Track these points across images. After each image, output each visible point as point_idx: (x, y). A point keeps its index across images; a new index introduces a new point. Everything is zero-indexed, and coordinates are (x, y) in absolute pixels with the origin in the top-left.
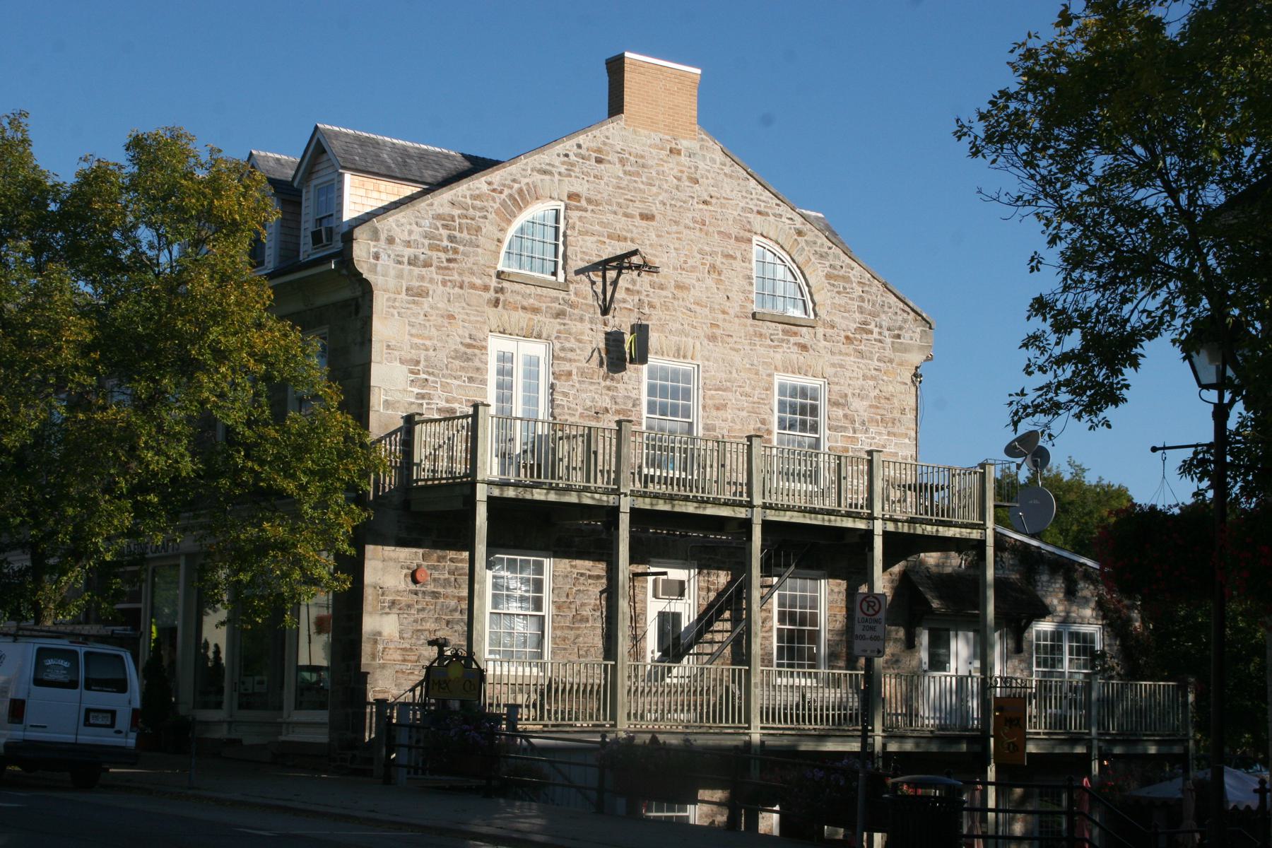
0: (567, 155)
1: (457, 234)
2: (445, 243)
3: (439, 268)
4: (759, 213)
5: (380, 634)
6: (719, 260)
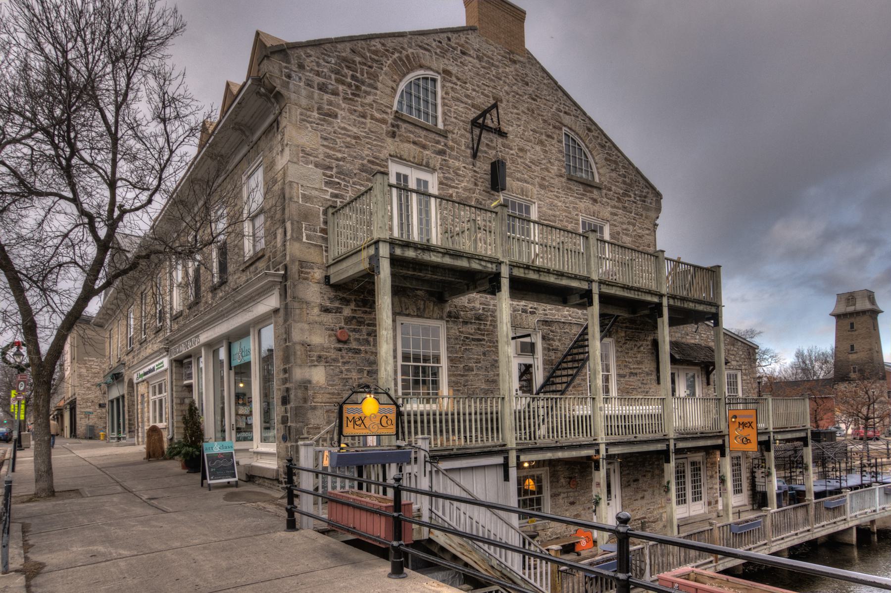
0: (440, 42)
1: (358, 75)
2: (349, 80)
3: (345, 99)
4: (565, 113)
5: (310, 382)
6: (544, 137)
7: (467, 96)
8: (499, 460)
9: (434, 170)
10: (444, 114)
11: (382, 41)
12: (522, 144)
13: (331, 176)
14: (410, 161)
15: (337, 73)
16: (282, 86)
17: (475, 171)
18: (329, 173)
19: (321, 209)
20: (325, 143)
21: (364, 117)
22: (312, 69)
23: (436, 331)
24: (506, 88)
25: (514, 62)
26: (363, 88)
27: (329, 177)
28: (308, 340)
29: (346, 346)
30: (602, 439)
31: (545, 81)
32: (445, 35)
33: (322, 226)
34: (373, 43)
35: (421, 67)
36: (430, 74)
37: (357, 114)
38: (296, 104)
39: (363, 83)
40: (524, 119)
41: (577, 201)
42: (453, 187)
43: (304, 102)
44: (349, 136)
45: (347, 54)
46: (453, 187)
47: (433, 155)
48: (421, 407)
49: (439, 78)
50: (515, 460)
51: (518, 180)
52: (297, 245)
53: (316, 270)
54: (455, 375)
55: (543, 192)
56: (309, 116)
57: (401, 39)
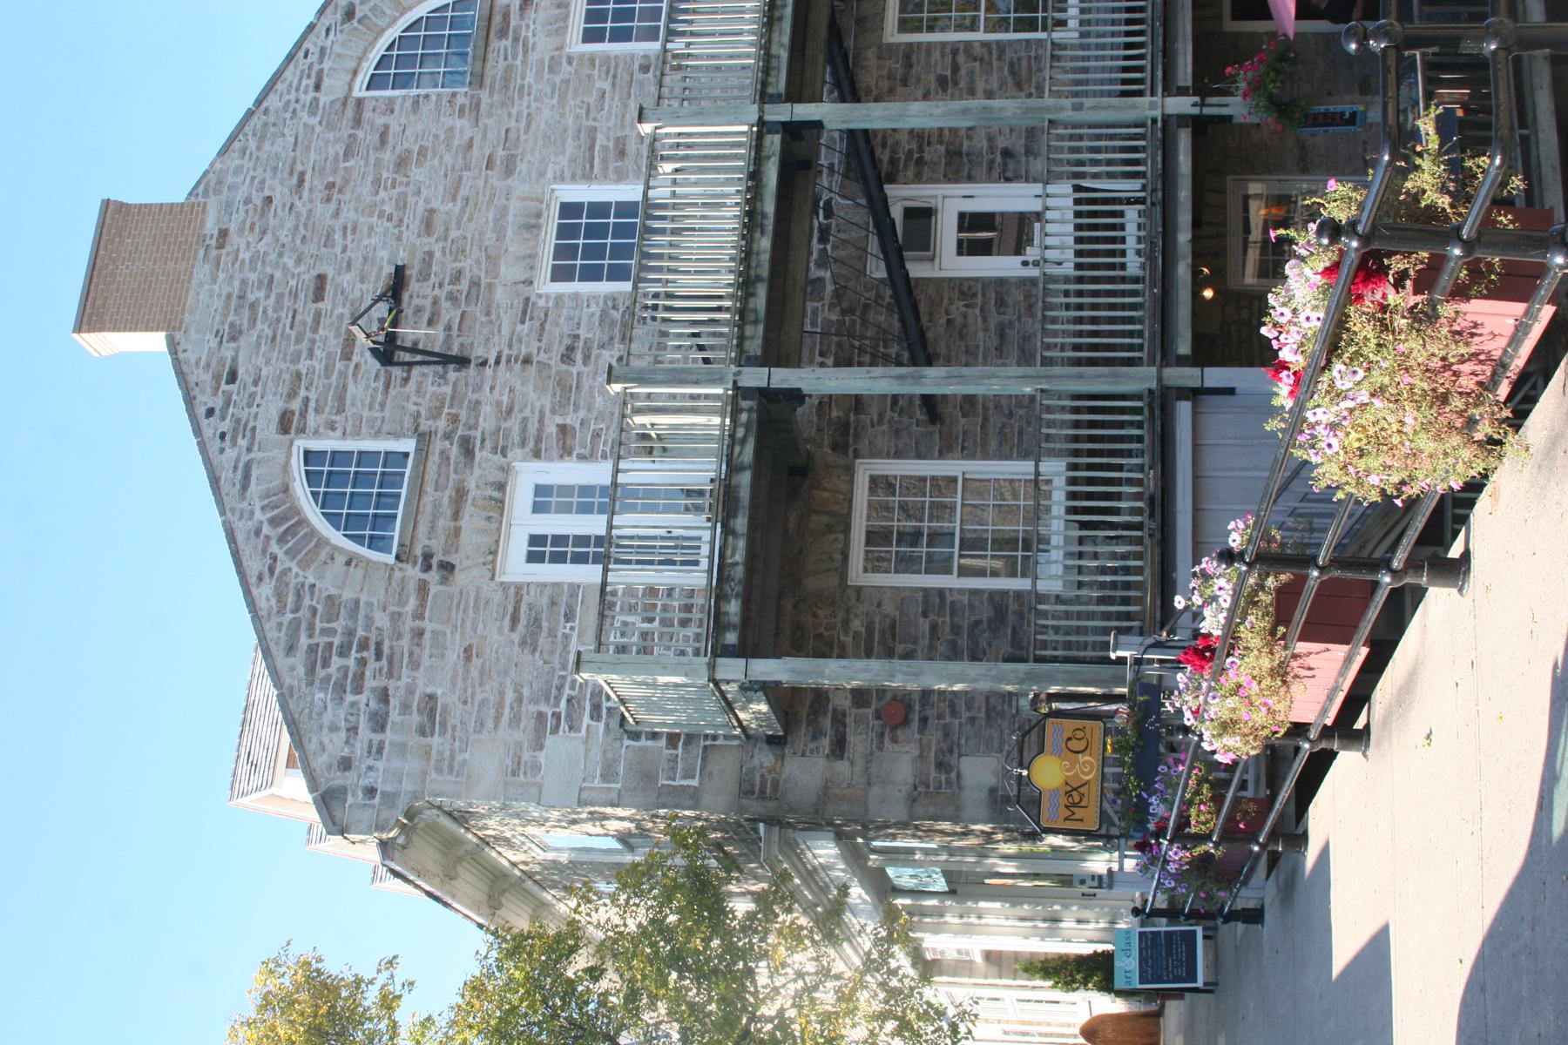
0: (223, 436)
1: (337, 641)
2: (351, 662)
3: (390, 675)
4: (317, 87)
5: (993, 791)
6: (388, 156)
7: (328, 371)
8: (1184, 409)
9: (506, 470)
10: (377, 434)
11: (254, 580)
12: (413, 225)
13: (557, 716)
14: (499, 529)
15: (340, 688)
16: (392, 806)
17: (497, 362)
18: (550, 721)
19: (627, 742)
20: (490, 724)
21: (420, 633)
22: (347, 742)
23: (879, 484)
24: (289, 262)
25: (223, 234)
26: (360, 633)
27: (559, 719)
28: (905, 789)
29: (917, 707)
30: (1152, 106)
31: (253, 144)
32: (204, 422)
33: (663, 742)
34: (262, 604)
35: (286, 489)
36: (297, 466)
37: (417, 650)
38: (424, 781)
39: (350, 633)
40: (352, 215)
41: (533, 57)
42: (541, 421)
43: (413, 764)
44: (467, 671)
45: (299, 661)
46: (541, 421)
47: (477, 472)
48: (1057, 555)
49: (302, 444)
50: (1188, 371)
51: (501, 236)
52: (707, 798)
53: (756, 762)
54: (985, 443)
55: (522, 167)
56: (440, 753)
57: (240, 537)
